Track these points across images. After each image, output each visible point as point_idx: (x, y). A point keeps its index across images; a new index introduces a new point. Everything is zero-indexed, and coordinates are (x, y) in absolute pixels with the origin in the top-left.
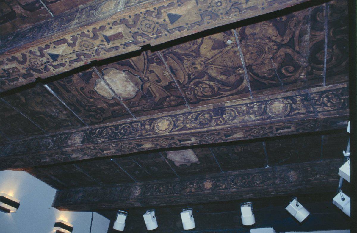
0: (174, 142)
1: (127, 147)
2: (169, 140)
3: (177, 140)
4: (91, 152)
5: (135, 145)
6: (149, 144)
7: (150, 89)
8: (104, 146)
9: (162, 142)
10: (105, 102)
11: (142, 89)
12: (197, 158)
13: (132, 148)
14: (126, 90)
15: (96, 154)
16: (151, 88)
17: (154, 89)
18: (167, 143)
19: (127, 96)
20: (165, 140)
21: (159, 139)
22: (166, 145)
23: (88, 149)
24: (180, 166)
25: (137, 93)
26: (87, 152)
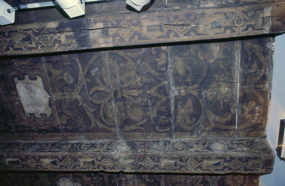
0: (22, 162)
1: (66, 163)
2: (26, 165)
3: (20, 163)
4: (106, 163)
5: (58, 164)
6: (44, 163)
7: (48, 180)
8: (88, 167)
9: (33, 164)
10: (83, 181)
11: (54, 182)
12: (18, 90)
13: (61, 161)
14: (65, 184)
15: (101, 160)
16: (48, 181)
17: (46, 179)
18: (29, 161)
19: (66, 179)
20: (30, 165)
21: (34, 168)
22: (30, 158)
23: (107, 167)
24: (37, 76)
25: (58, 180)
26: (110, 164)
